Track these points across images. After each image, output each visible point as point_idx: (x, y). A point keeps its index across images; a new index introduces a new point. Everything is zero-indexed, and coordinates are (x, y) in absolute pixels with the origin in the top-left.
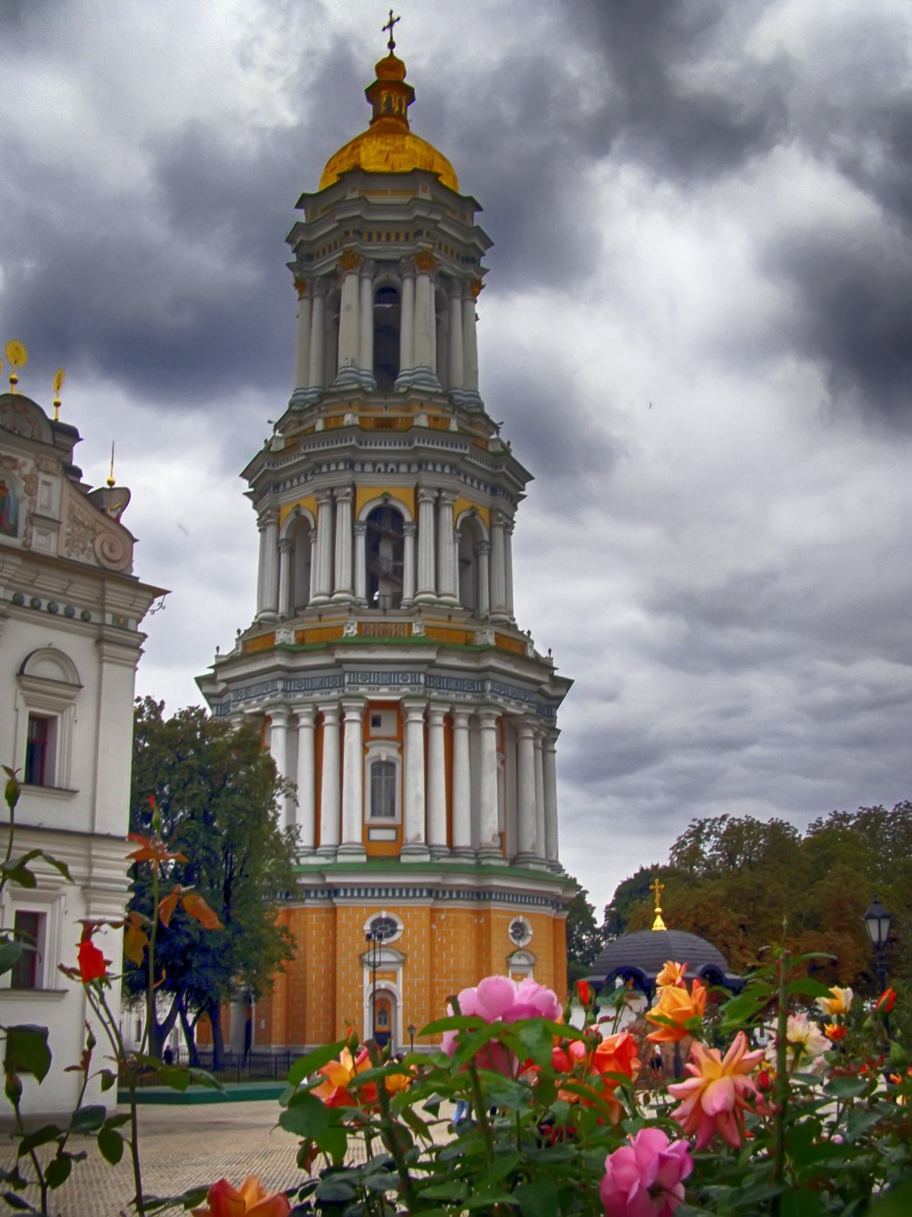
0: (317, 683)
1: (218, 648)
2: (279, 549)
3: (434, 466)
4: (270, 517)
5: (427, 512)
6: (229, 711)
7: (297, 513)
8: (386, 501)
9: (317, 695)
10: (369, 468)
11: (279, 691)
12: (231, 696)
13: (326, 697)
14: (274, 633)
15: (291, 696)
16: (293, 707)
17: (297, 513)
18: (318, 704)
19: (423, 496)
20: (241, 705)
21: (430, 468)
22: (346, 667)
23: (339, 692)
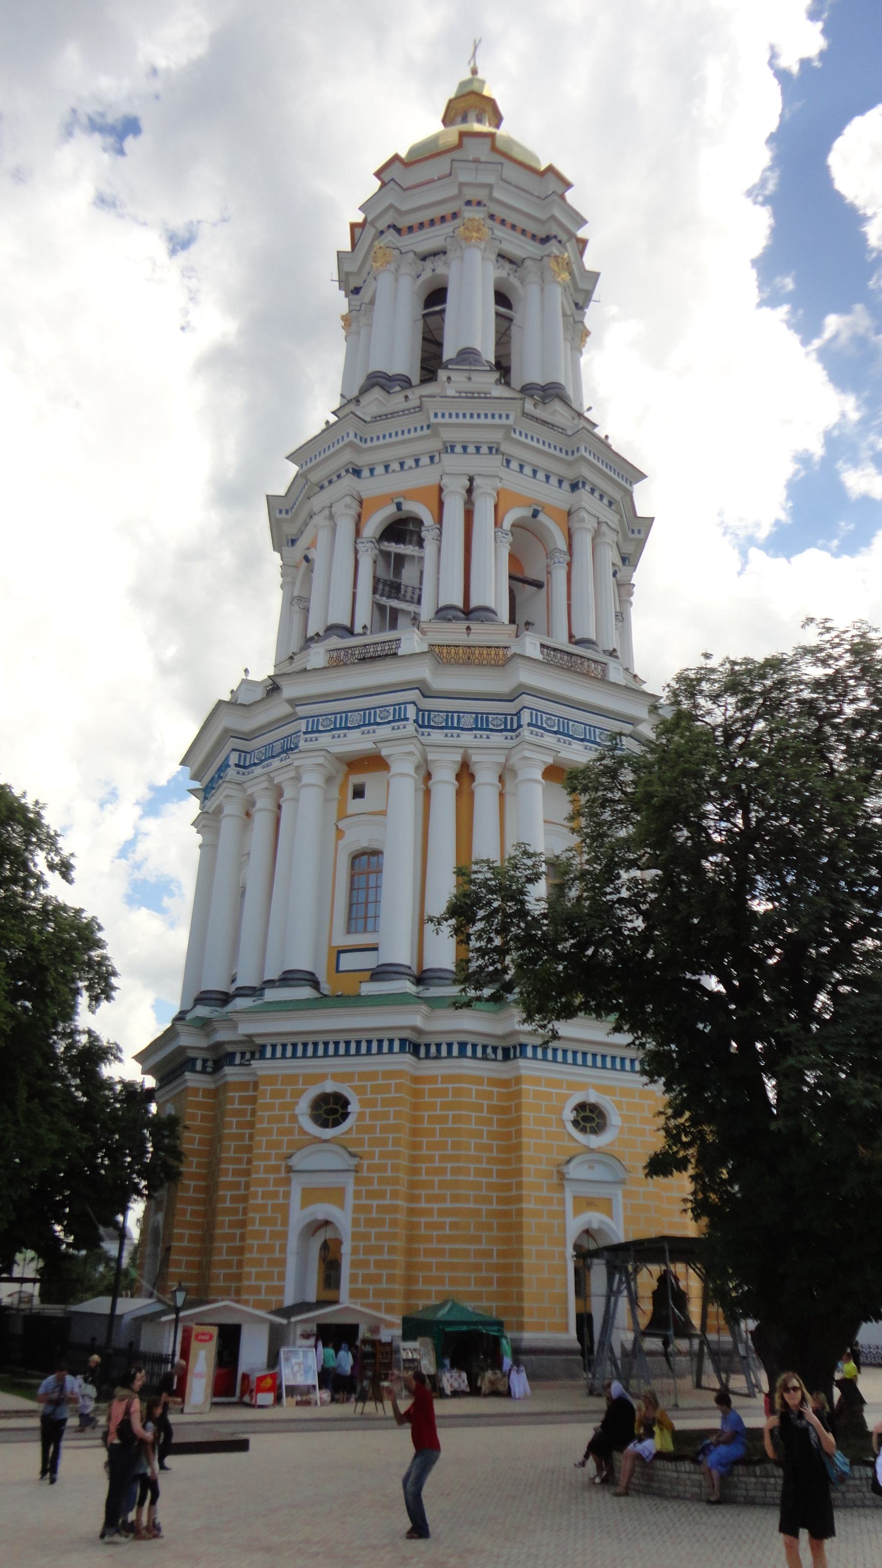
0: (468, 721)
1: (246, 671)
2: (356, 552)
3: (593, 491)
4: (347, 506)
5: (584, 542)
6: (297, 747)
7: (399, 506)
8: (535, 514)
9: (467, 738)
10: (514, 465)
11: (411, 721)
12: (302, 725)
13: (483, 742)
14: (399, 640)
15: (423, 734)
16: (428, 749)
17: (399, 506)
18: (470, 751)
19: (582, 520)
20: (324, 740)
21: (588, 488)
22: (526, 700)
23: (506, 738)
